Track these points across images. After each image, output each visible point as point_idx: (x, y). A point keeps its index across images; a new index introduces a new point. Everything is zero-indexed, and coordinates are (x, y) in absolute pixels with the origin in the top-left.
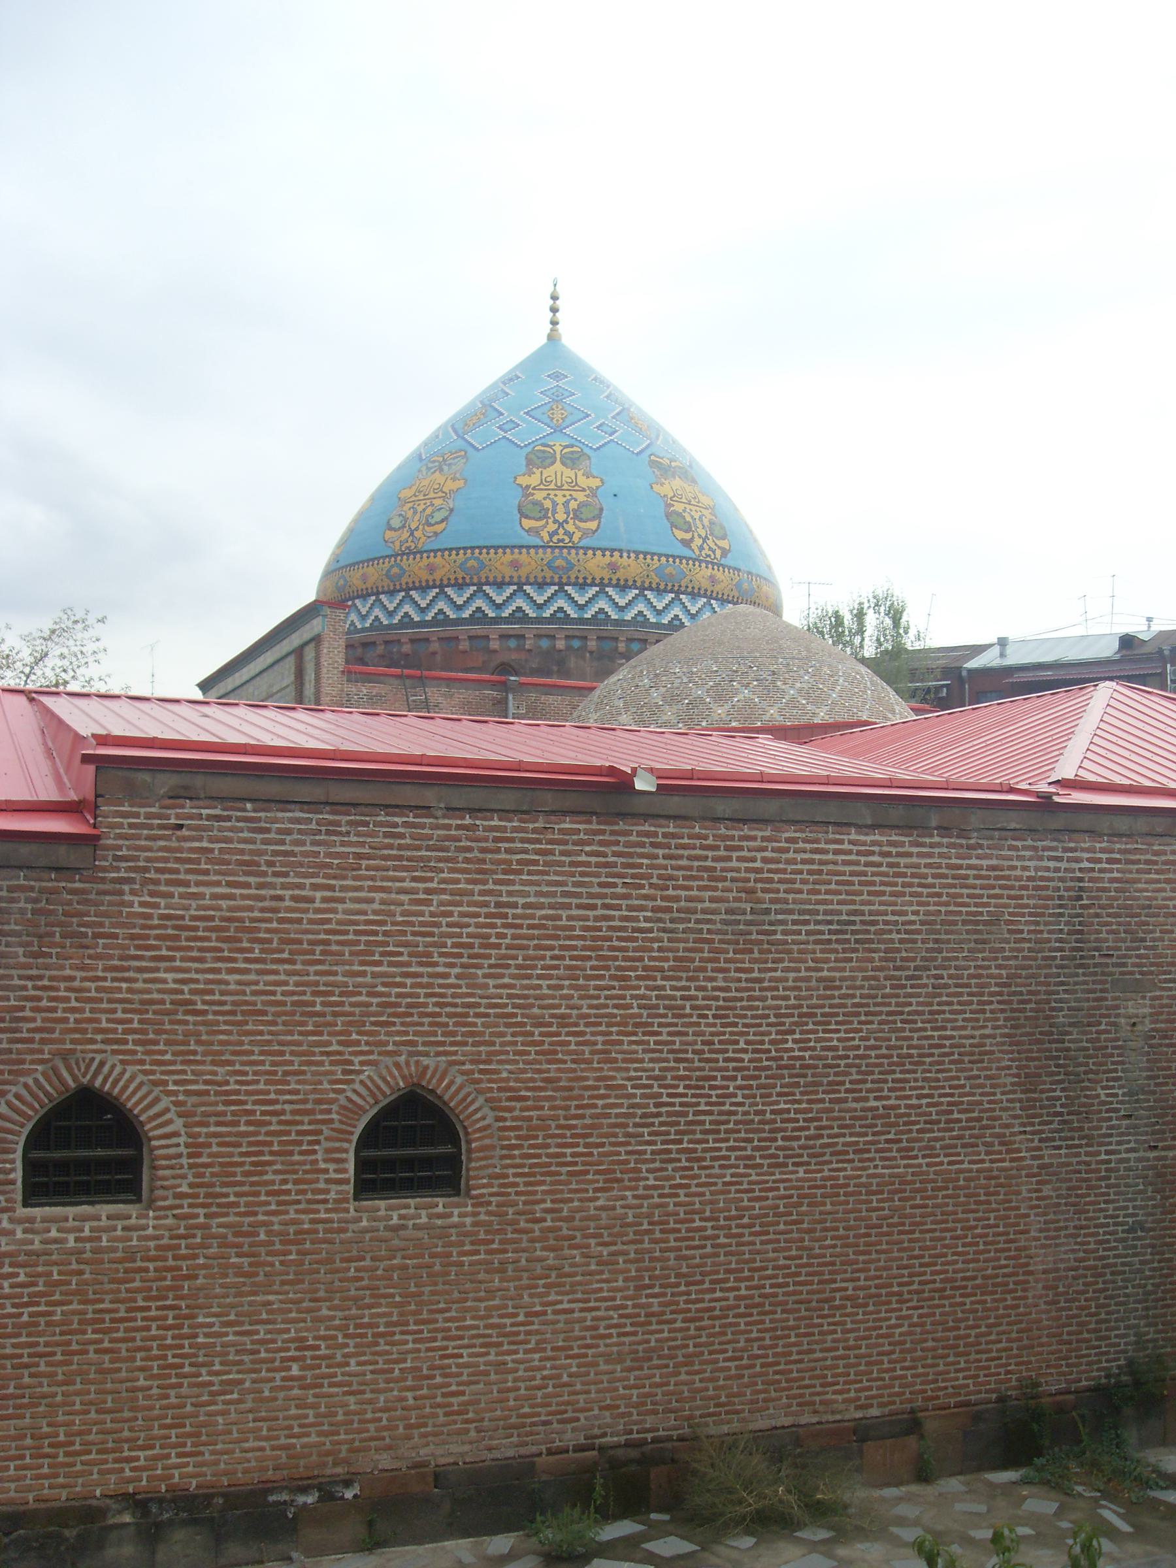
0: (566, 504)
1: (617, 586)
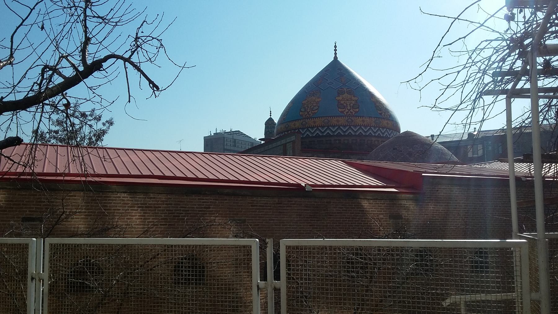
0: (350, 104)
1: (364, 126)
